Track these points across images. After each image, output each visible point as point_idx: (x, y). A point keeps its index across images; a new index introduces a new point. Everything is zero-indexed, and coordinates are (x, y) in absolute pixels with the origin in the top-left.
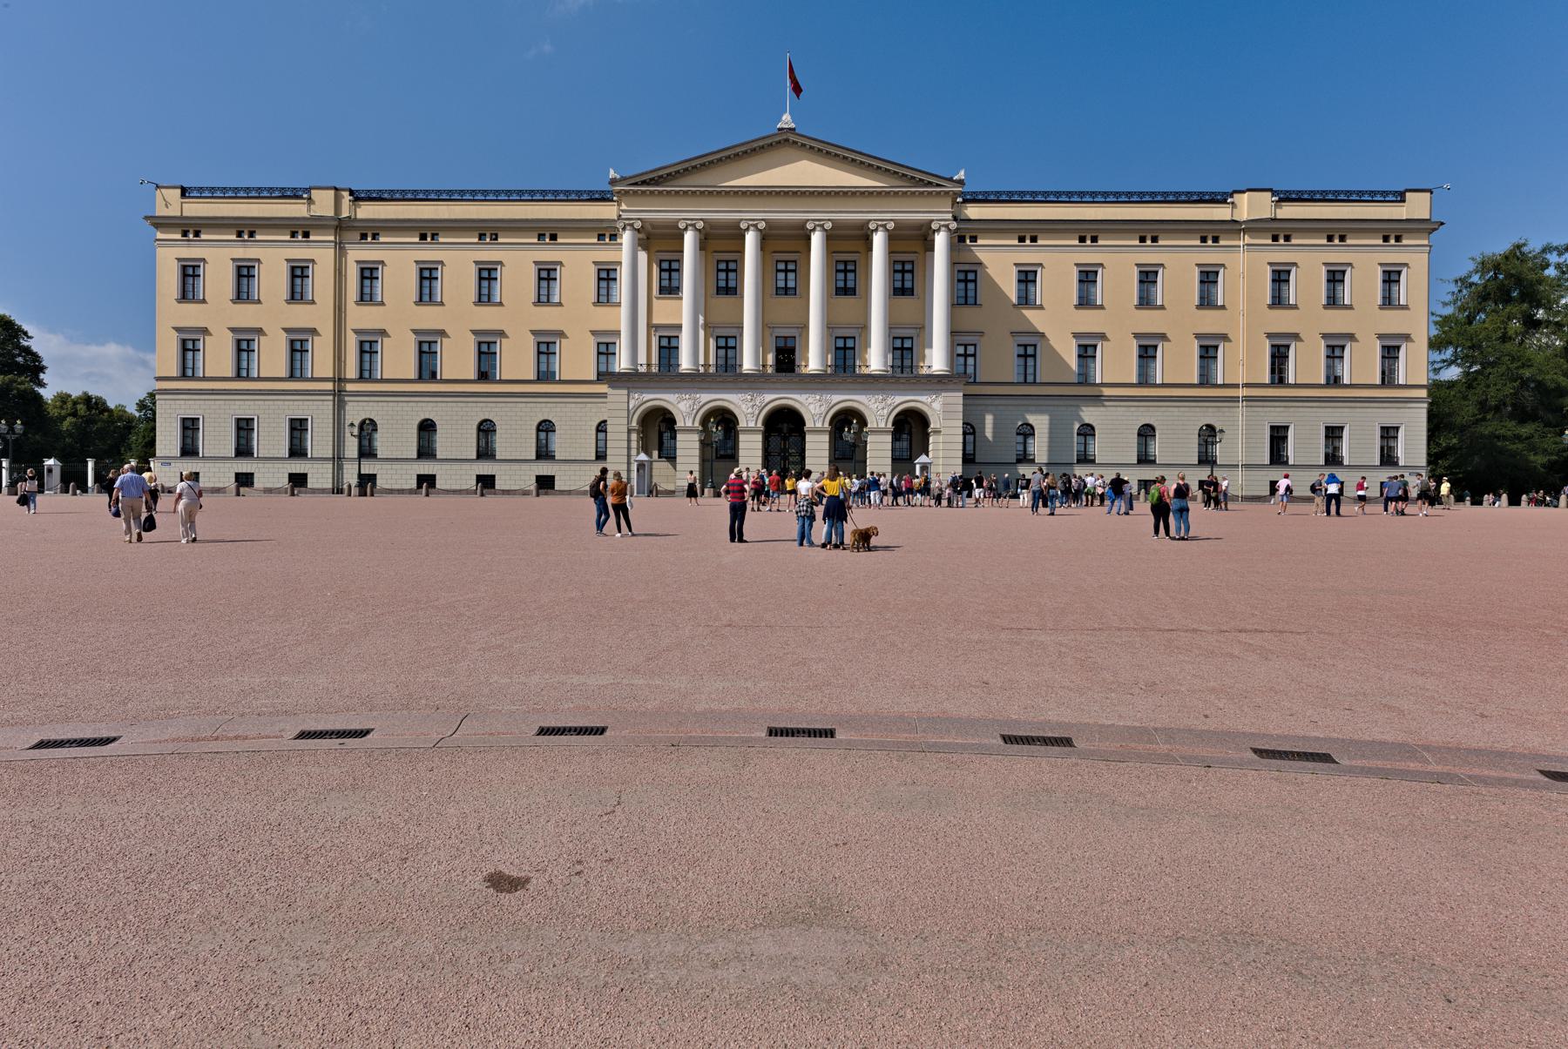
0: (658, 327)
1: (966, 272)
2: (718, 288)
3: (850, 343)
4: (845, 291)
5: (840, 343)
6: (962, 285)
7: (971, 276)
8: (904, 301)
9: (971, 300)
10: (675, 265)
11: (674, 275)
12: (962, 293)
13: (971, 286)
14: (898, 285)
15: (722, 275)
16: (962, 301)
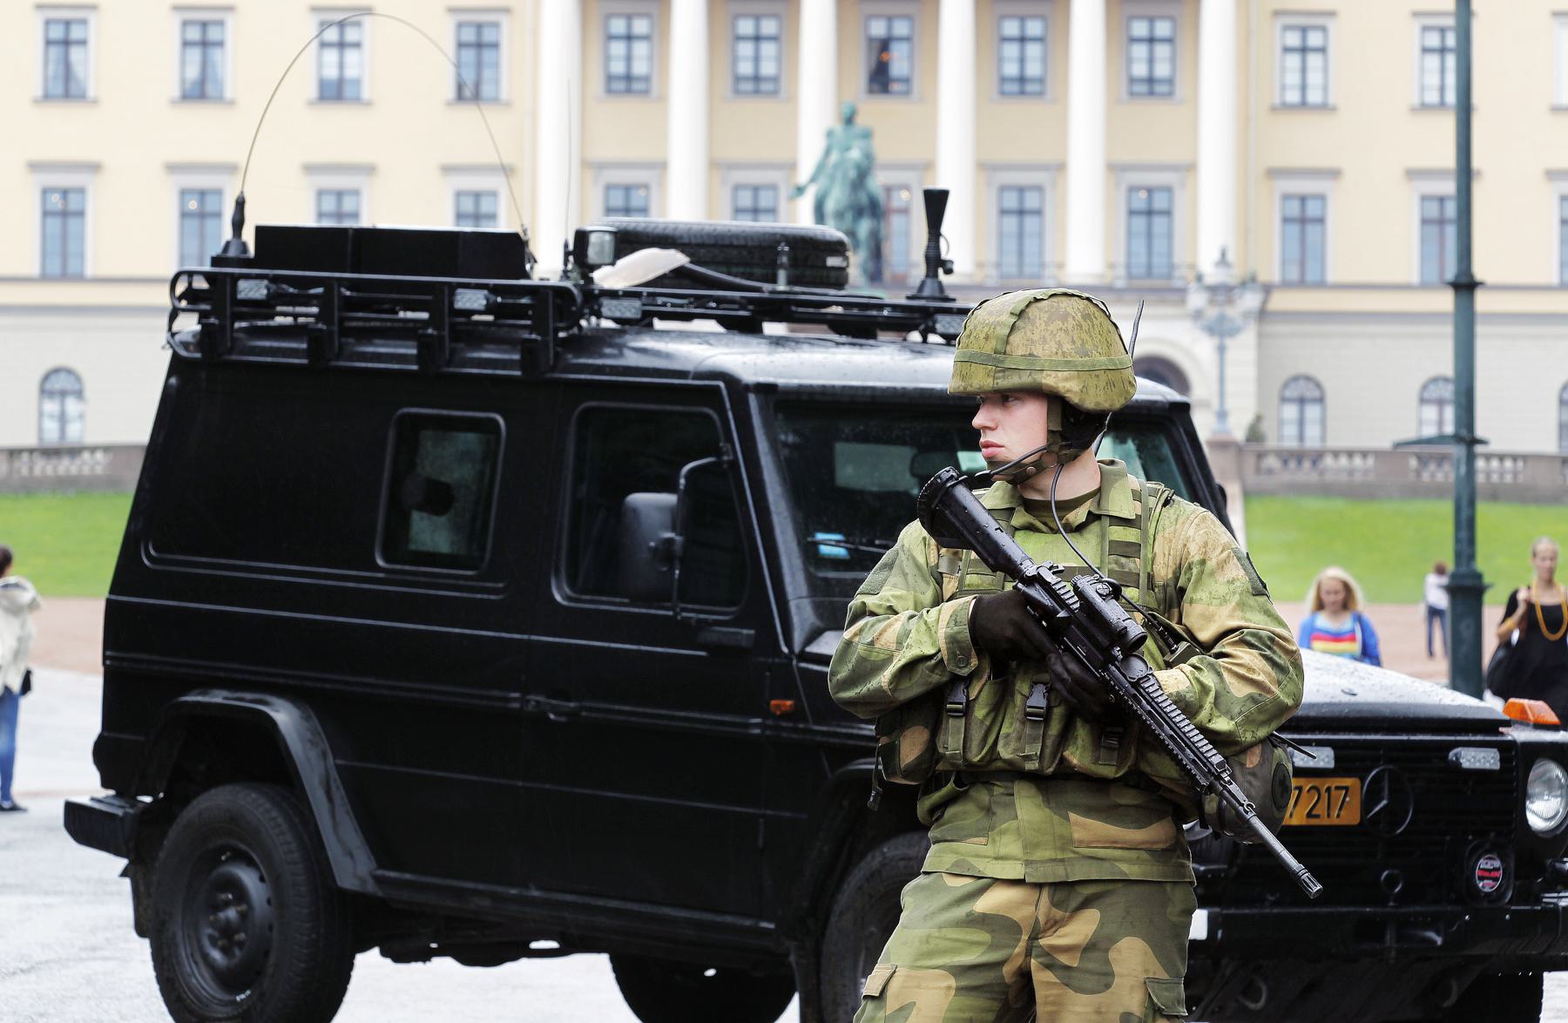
0: (601, 166)
1: (1304, 30)
2: (738, 79)
3: (1031, 201)
4: (1022, 86)
5: (1011, 201)
6: (1293, 61)
7: (1314, 39)
8: (1154, 112)
9: (1314, 97)
10: (640, 26)
11: (640, 49)
12: (1293, 79)
13: (1314, 60)
14: (1140, 70)
15: (746, 49)
16: (1293, 97)
